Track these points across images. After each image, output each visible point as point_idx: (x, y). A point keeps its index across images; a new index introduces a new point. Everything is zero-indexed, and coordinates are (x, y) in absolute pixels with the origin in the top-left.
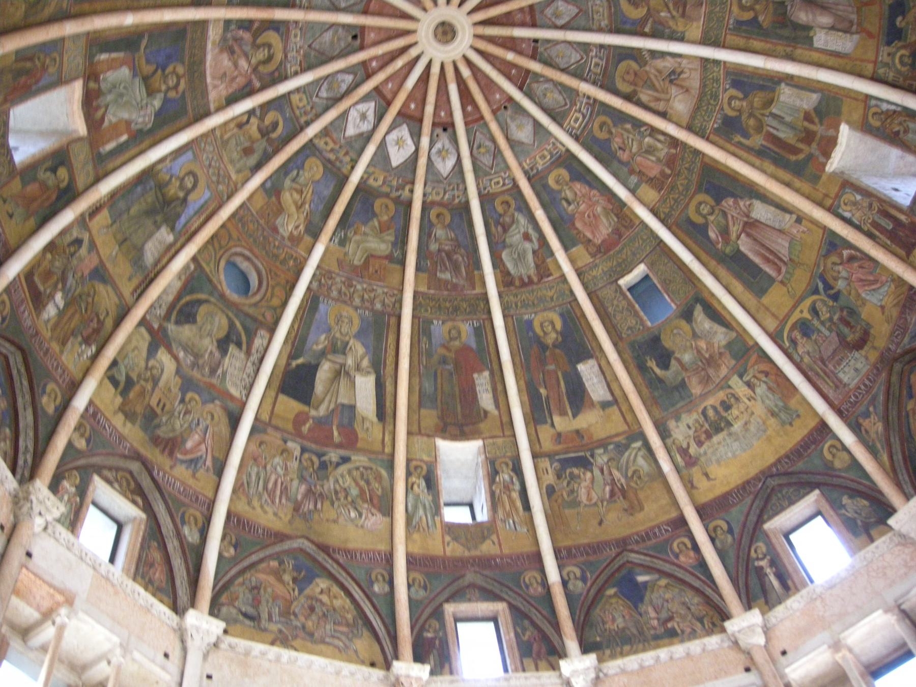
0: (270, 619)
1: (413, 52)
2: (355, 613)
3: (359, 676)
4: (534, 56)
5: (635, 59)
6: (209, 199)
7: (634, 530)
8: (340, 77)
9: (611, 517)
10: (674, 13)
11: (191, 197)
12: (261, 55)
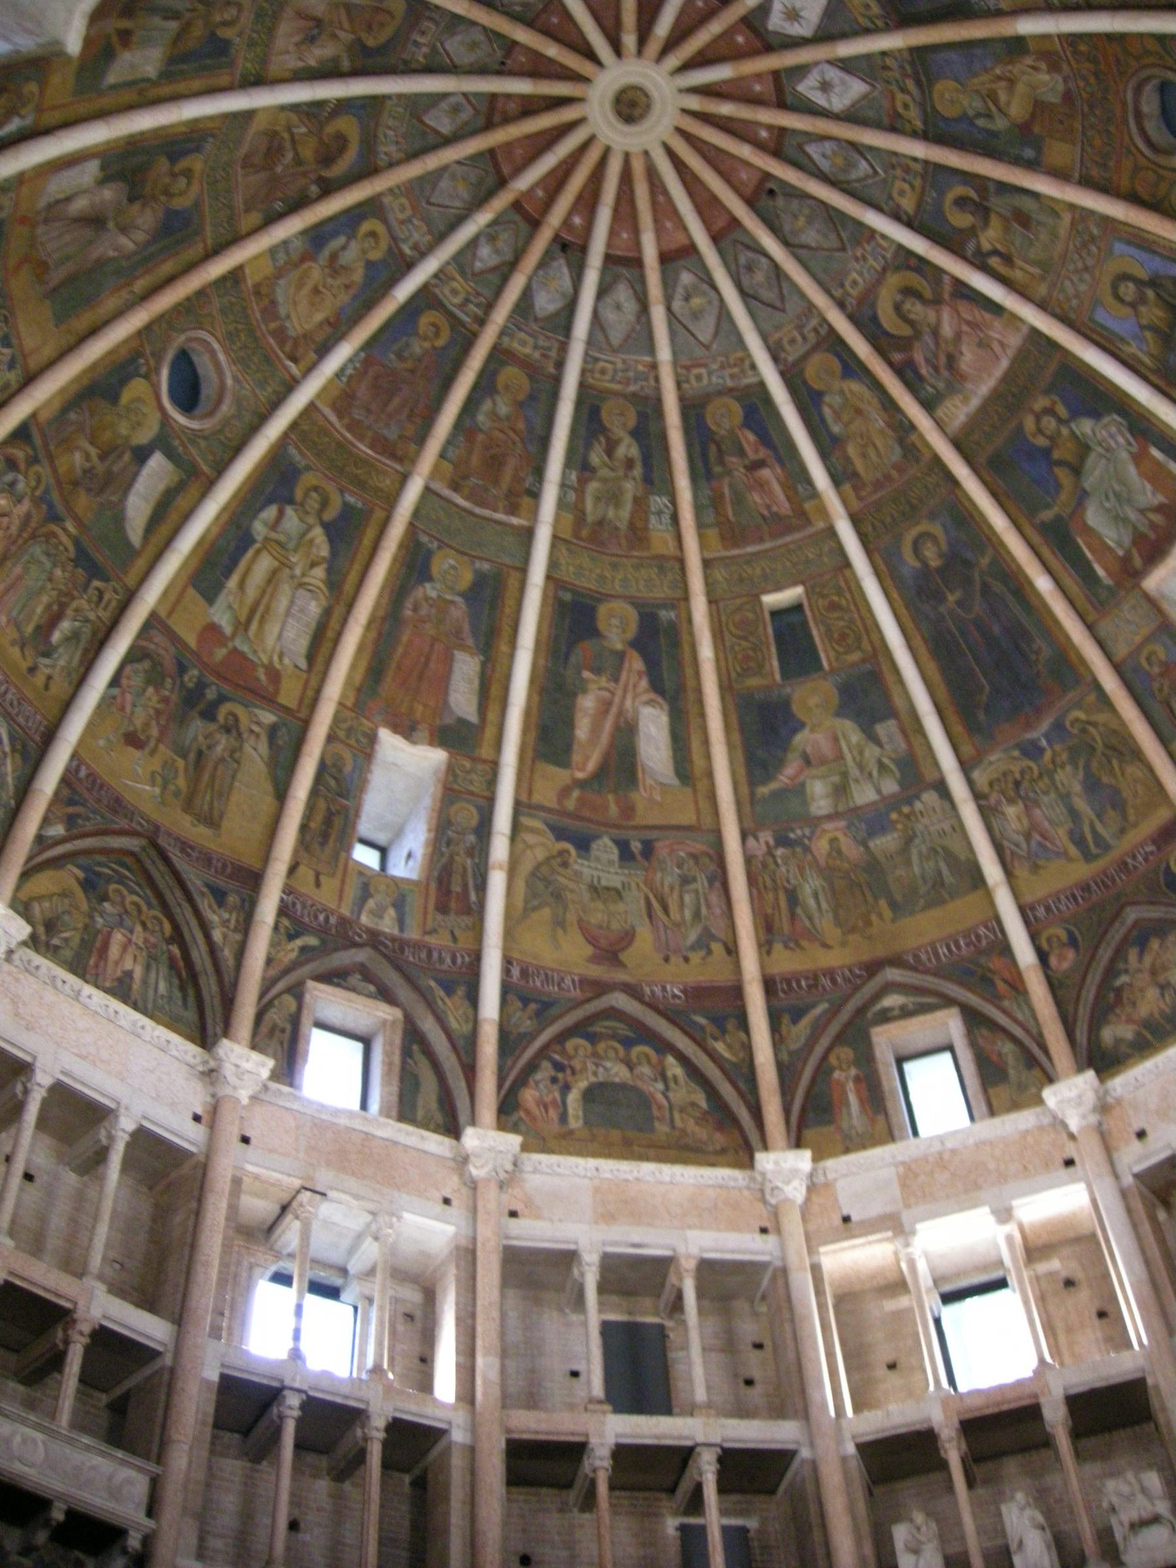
1: (694, 103)
4: (515, 43)
5: (366, 51)
6: (1120, 240)
8: (825, 165)
10: (286, 136)
11: (1143, 274)
12: (916, 309)
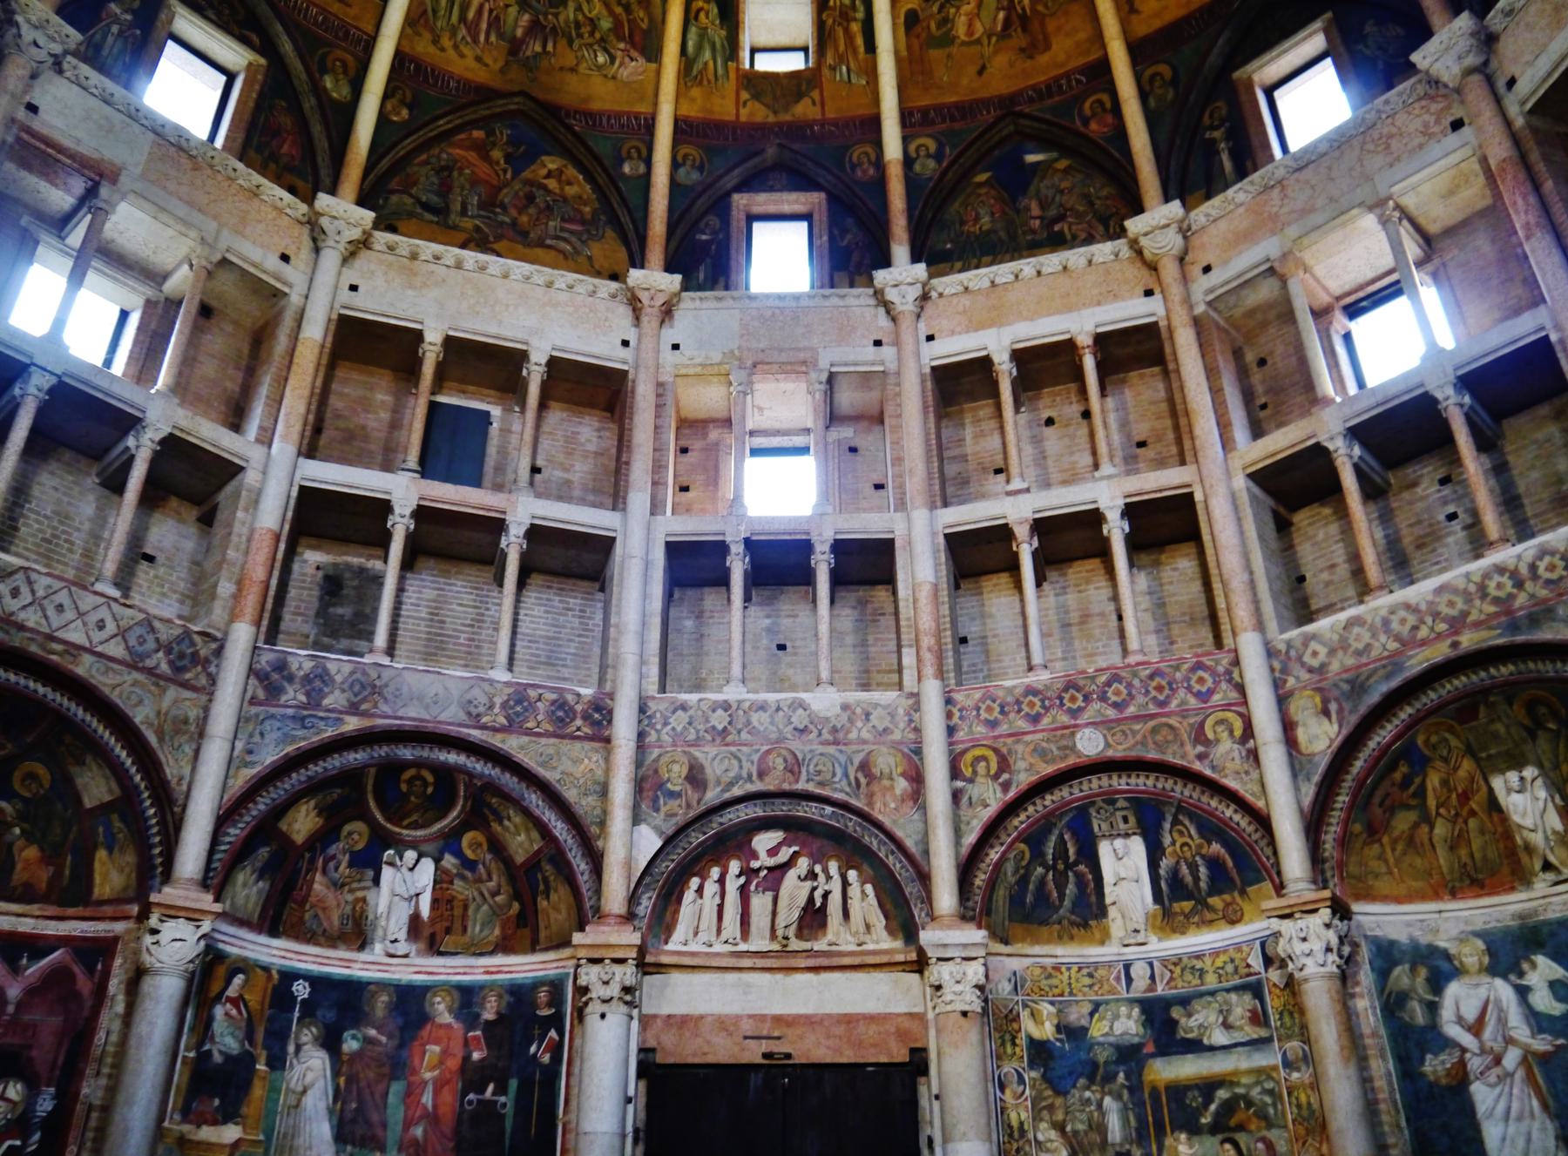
0: (464, 212)
2: (597, 205)
3: (580, 289)
7: (1031, 82)
9: (1000, 63)
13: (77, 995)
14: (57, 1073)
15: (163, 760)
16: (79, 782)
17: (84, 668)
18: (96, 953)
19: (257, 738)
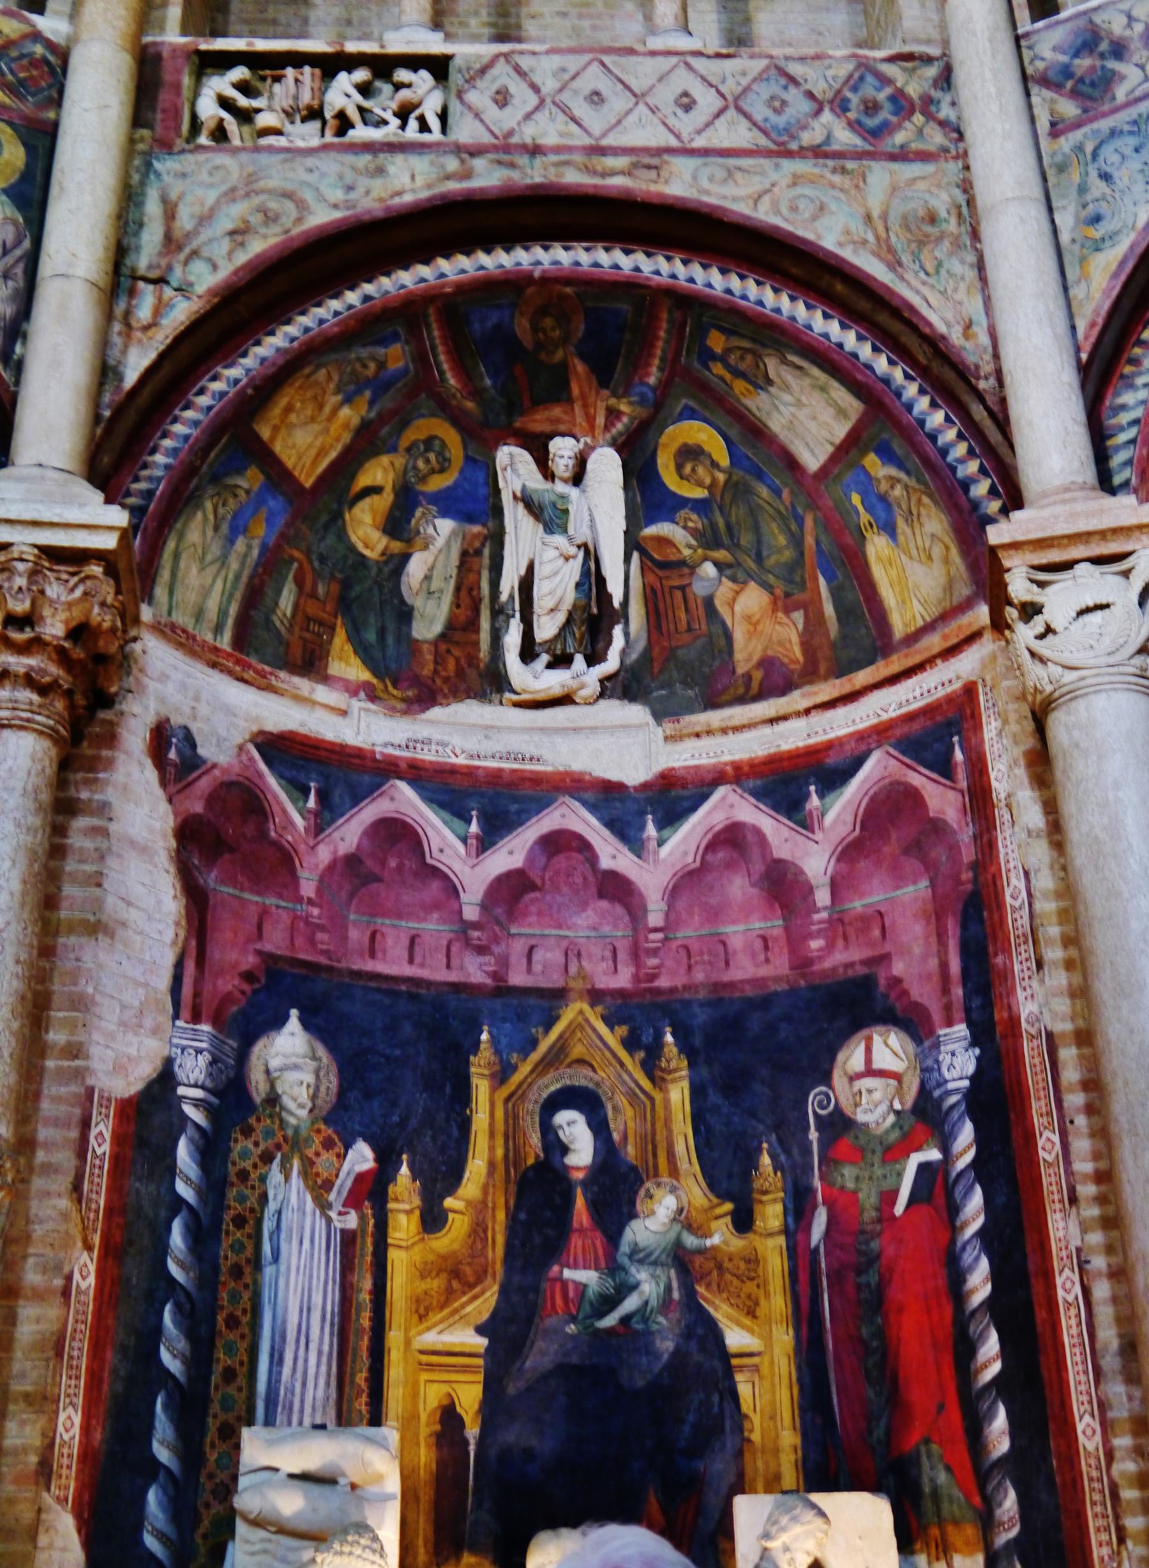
13: (937, 828)
14: (958, 992)
15: (916, 301)
16: (776, 424)
17: (681, 183)
18: (941, 736)
19: (1098, 187)
